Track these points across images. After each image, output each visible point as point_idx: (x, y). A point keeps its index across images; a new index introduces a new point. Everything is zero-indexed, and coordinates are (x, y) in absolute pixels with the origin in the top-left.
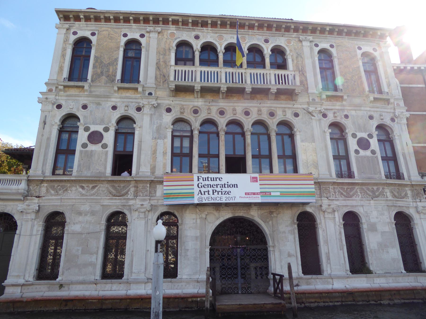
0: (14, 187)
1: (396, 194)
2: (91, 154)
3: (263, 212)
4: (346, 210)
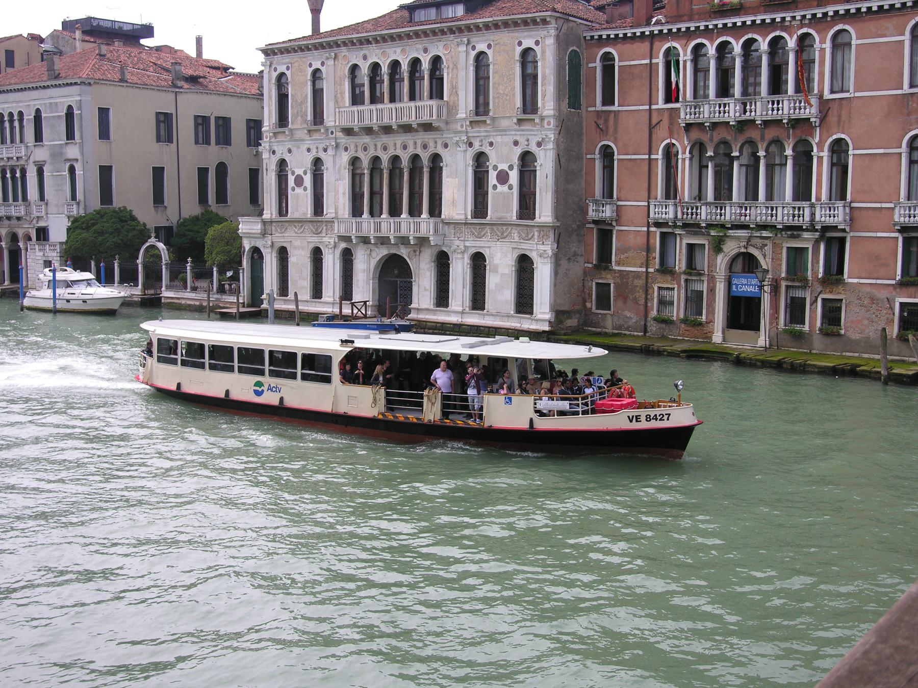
2: (297, 197)
4: (474, 250)
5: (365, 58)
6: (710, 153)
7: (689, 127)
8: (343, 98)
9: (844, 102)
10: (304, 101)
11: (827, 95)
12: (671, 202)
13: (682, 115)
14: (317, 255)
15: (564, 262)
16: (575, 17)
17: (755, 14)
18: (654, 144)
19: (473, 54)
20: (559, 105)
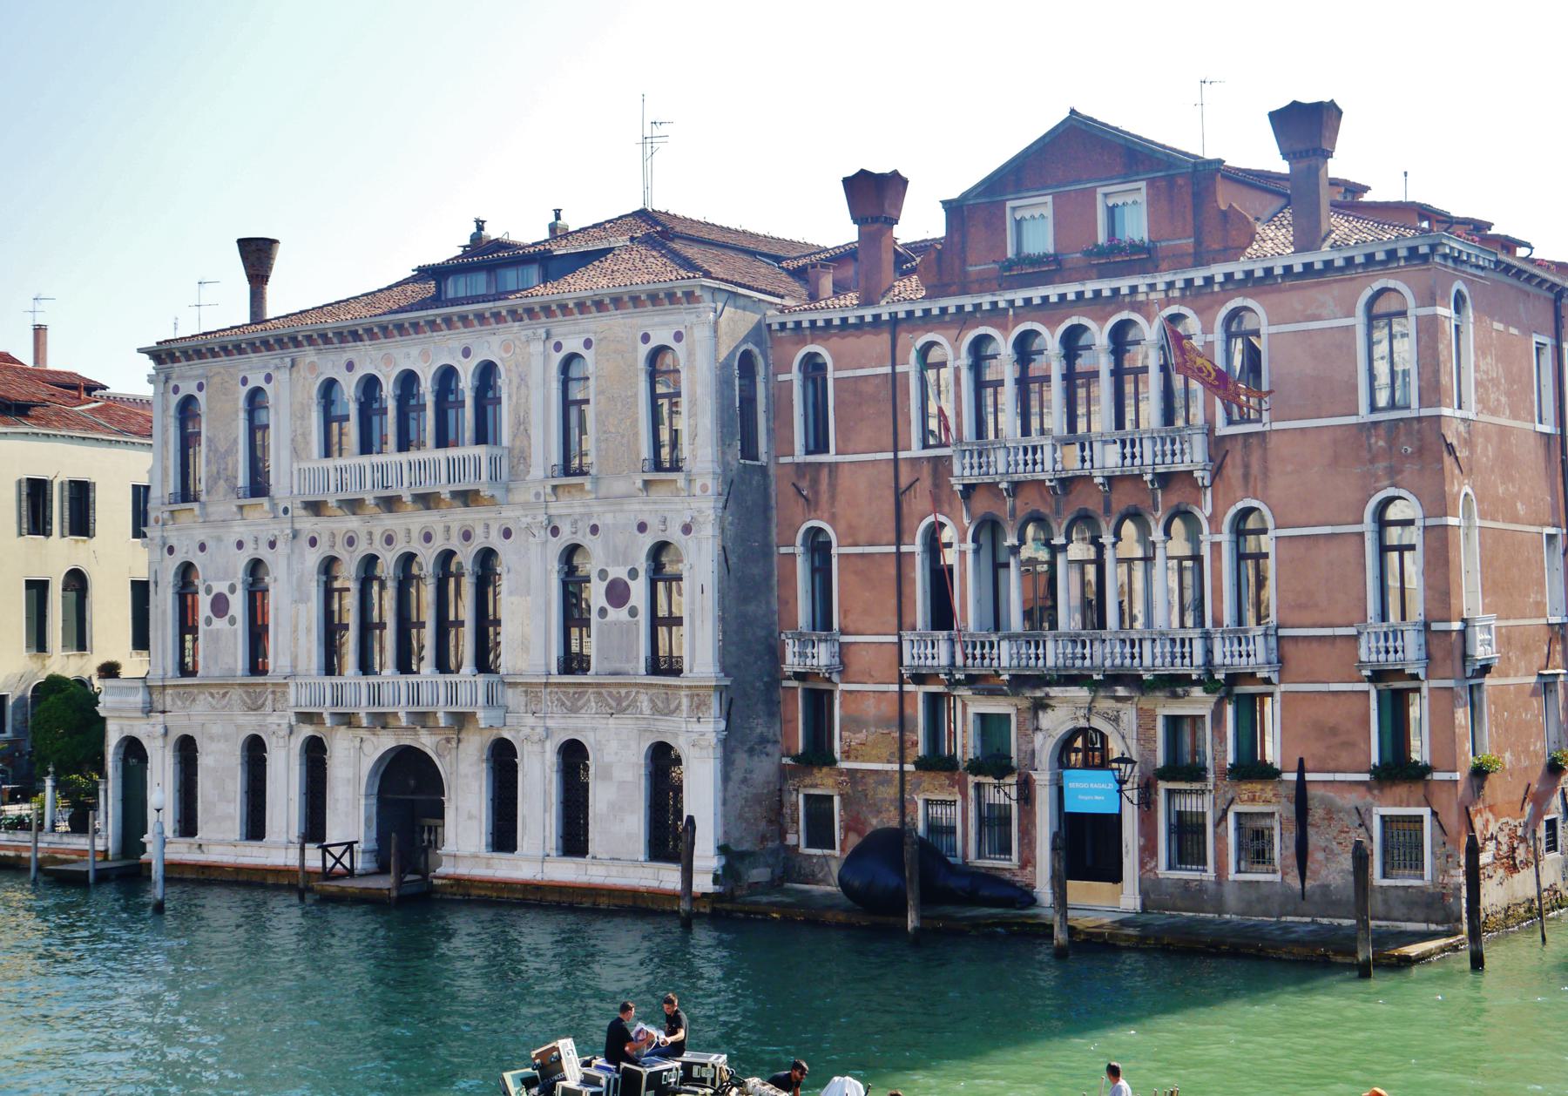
0: (131, 699)
1: (660, 705)
2: (215, 637)
3: (438, 738)
5: (350, 366)
6: (1011, 540)
7: (969, 489)
8: (307, 443)
9: (1252, 440)
10: (231, 450)
11: (1222, 429)
12: (942, 635)
13: (957, 470)
14: (255, 751)
15: (741, 758)
16: (749, 288)
17: (1082, 279)
18: (906, 524)
19: (558, 358)
20: (723, 453)
